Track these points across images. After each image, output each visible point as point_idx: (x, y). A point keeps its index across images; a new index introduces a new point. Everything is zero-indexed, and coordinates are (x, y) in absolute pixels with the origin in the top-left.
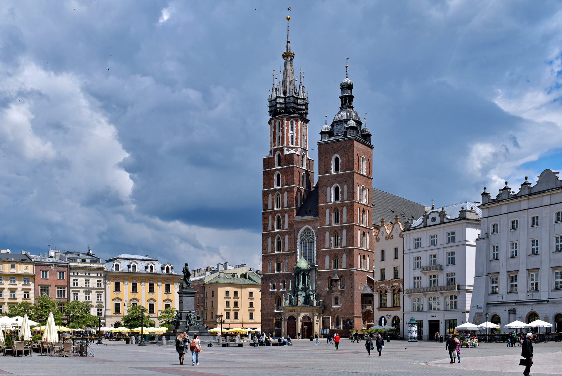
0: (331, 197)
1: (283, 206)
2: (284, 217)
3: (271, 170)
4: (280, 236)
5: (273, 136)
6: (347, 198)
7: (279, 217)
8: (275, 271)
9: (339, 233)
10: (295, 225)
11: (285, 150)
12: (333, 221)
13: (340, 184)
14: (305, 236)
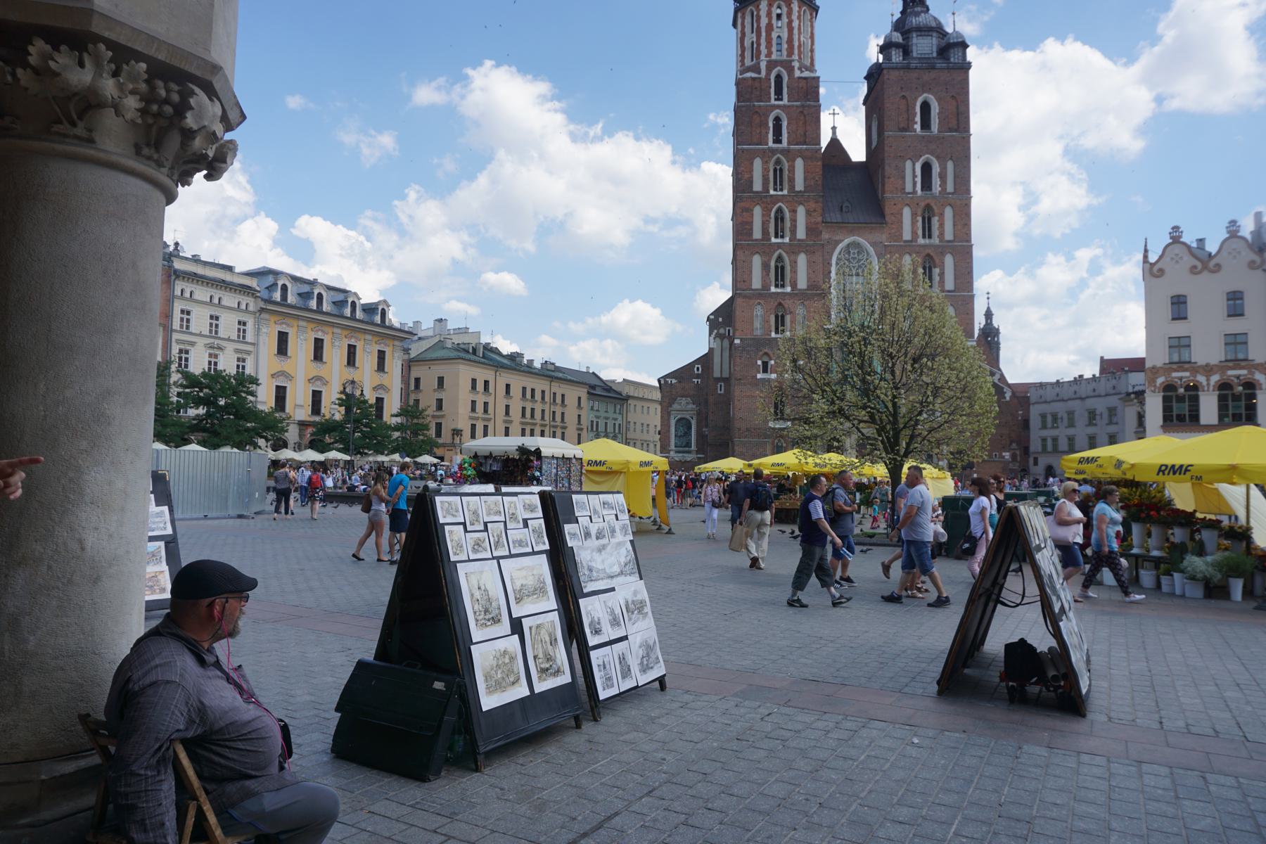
0: (915, 184)
1: (792, 187)
2: (794, 211)
3: (760, 106)
4: (784, 254)
5: (764, 34)
6: (955, 189)
7: (780, 210)
8: (771, 331)
9: (937, 261)
10: (823, 233)
11: (796, 68)
12: (920, 232)
13: (938, 158)
14: (848, 260)
